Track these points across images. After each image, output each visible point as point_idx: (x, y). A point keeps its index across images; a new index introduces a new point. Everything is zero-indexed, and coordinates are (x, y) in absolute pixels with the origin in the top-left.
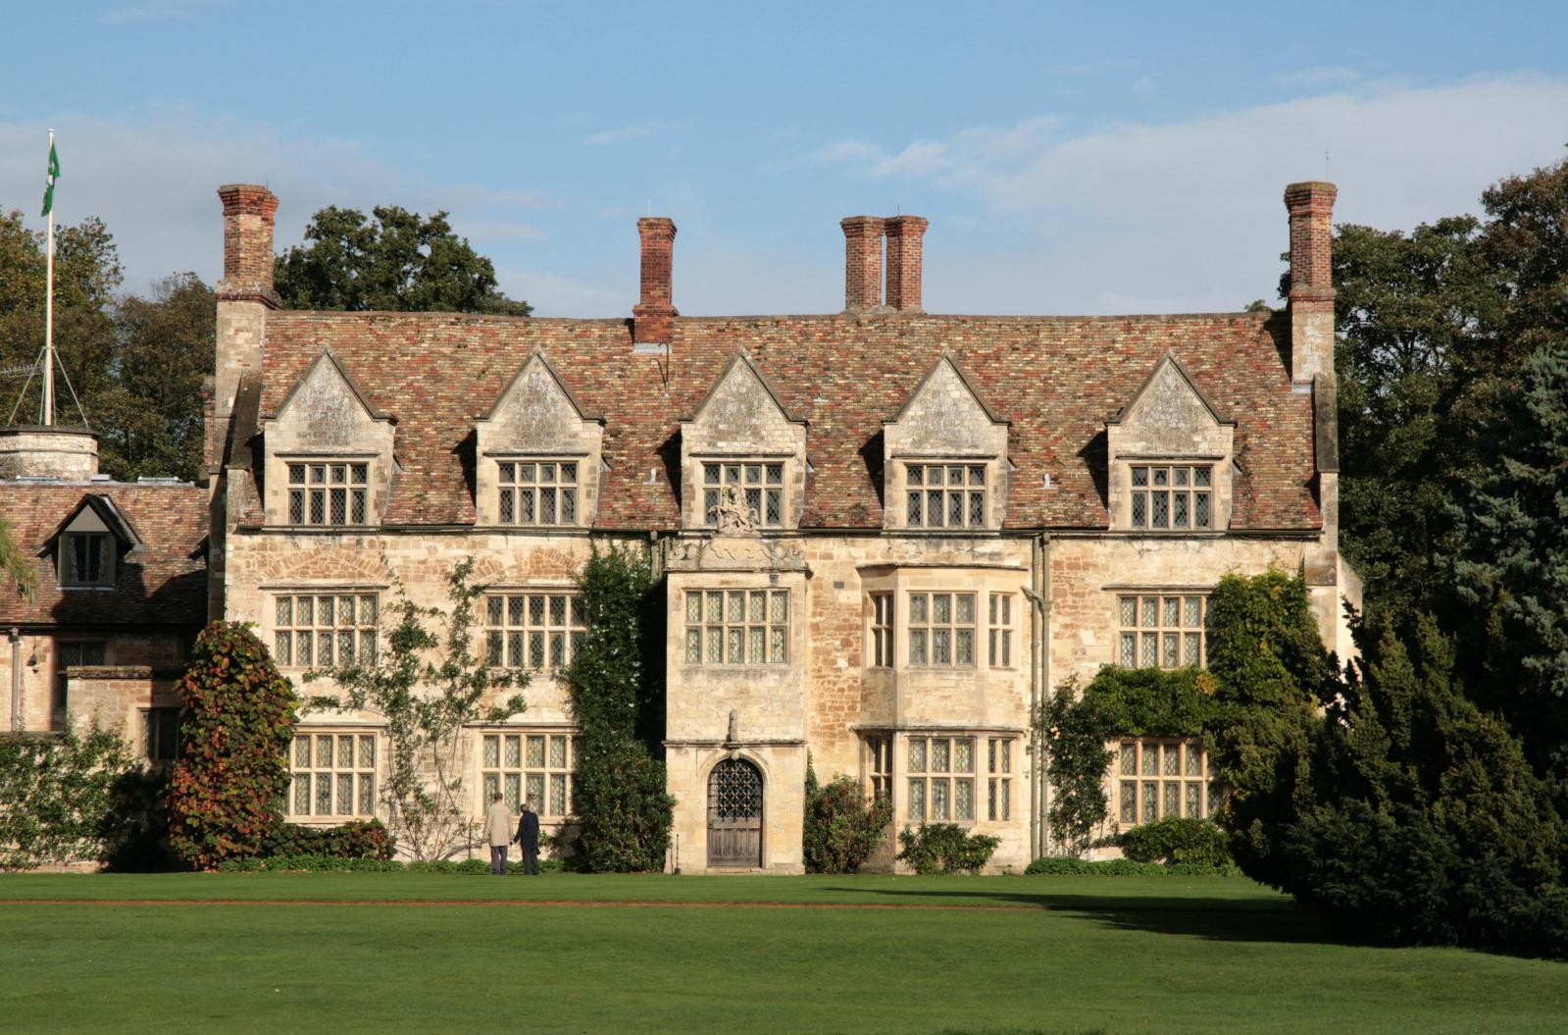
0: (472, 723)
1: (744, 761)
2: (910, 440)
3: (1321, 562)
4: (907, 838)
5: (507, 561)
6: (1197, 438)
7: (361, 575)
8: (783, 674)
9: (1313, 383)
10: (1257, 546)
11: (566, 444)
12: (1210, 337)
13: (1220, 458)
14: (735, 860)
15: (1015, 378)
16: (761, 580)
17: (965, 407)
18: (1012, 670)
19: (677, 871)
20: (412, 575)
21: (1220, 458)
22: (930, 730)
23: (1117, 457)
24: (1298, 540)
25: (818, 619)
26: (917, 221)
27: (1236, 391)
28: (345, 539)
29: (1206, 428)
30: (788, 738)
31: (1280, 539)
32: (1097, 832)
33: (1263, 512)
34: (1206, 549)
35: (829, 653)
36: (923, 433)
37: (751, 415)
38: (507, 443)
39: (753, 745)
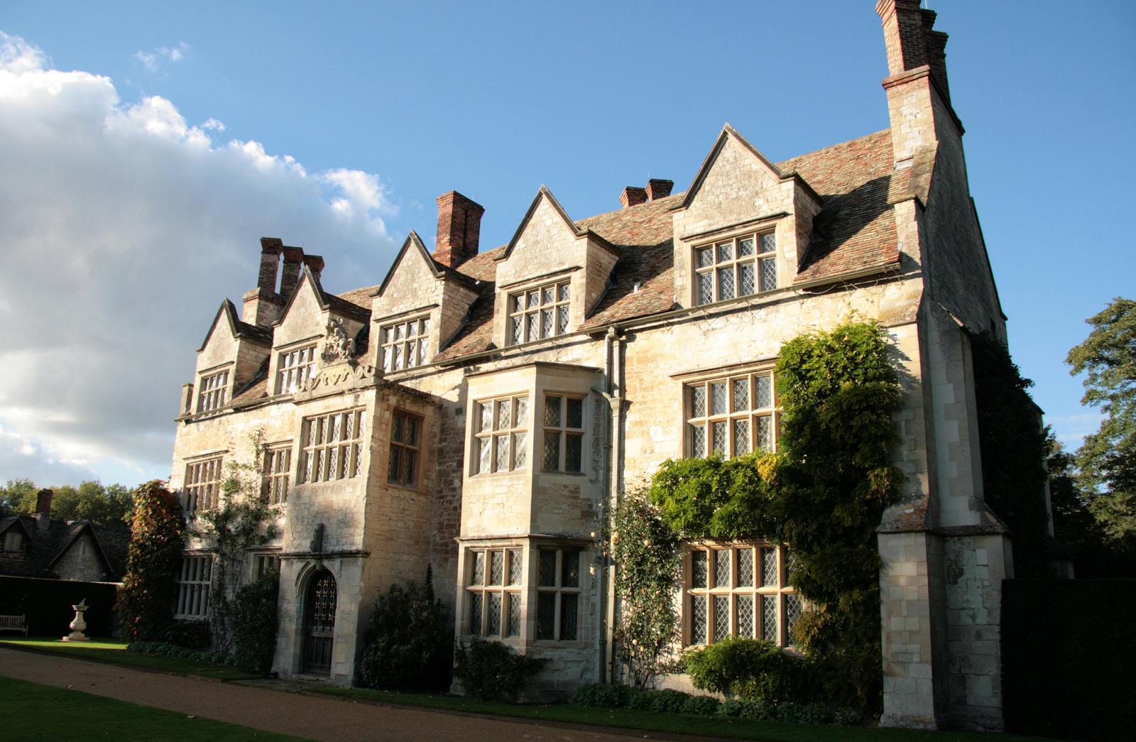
0: (253, 547)
1: (326, 574)
2: (514, 271)
3: (903, 303)
4: (462, 654)
5: (277, 424)
6: (759, 202)
7: (218, 445)
8: (354, 486)
9: (912, 158)
10: (826, 301)
11: (313, 331)
12: (829, 159)
13: (785, 215)
14: (321, 668)
15: (656, 229)
16: (348, 401)
17: (554, 231)
18: (583, 475)
19: (276, 675)
20: (237, 443)
21: (785, 215)
22: (481, 540)
23: (681, 239)
24: (881, 283)
25: (444, 444)
26: (664, 182)
27: (838, 185)
28: (217, 420)
29: (766, 190)
30: (353, 548)
31: (851, 288)
32: (663, 659)
33: (833, 265)
34: (772, 316)
35: (448, 474)
36: (523, 262)
37: (413, 280)
38: (285, 338)
39: (331, 556)
